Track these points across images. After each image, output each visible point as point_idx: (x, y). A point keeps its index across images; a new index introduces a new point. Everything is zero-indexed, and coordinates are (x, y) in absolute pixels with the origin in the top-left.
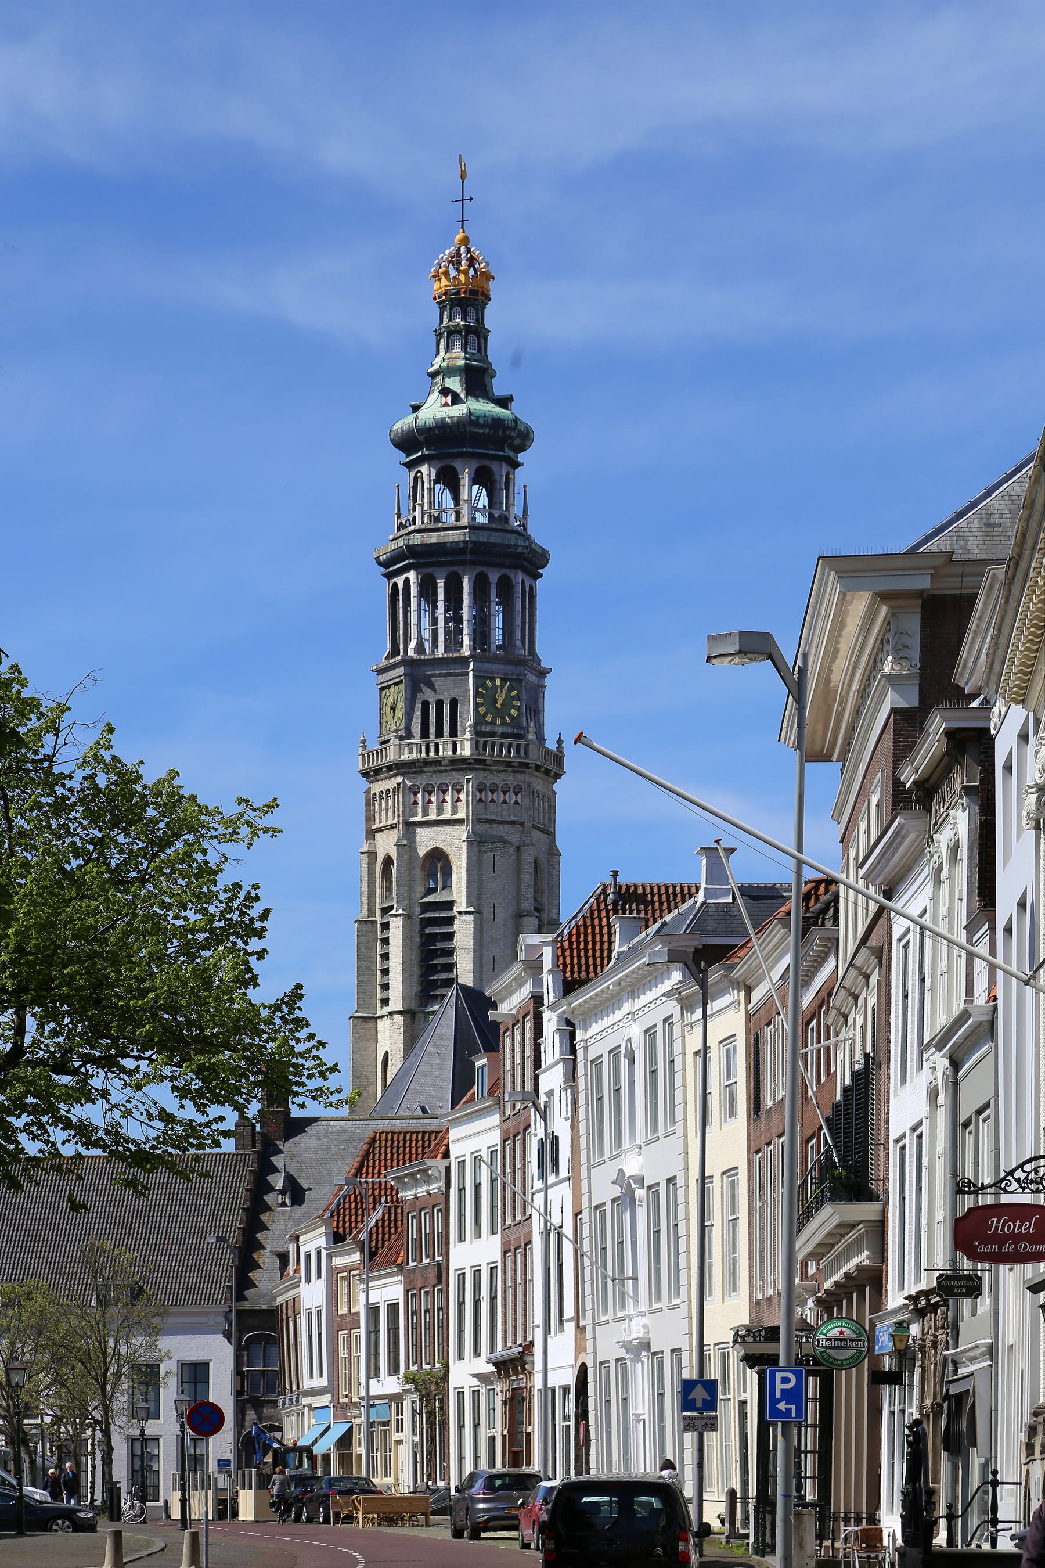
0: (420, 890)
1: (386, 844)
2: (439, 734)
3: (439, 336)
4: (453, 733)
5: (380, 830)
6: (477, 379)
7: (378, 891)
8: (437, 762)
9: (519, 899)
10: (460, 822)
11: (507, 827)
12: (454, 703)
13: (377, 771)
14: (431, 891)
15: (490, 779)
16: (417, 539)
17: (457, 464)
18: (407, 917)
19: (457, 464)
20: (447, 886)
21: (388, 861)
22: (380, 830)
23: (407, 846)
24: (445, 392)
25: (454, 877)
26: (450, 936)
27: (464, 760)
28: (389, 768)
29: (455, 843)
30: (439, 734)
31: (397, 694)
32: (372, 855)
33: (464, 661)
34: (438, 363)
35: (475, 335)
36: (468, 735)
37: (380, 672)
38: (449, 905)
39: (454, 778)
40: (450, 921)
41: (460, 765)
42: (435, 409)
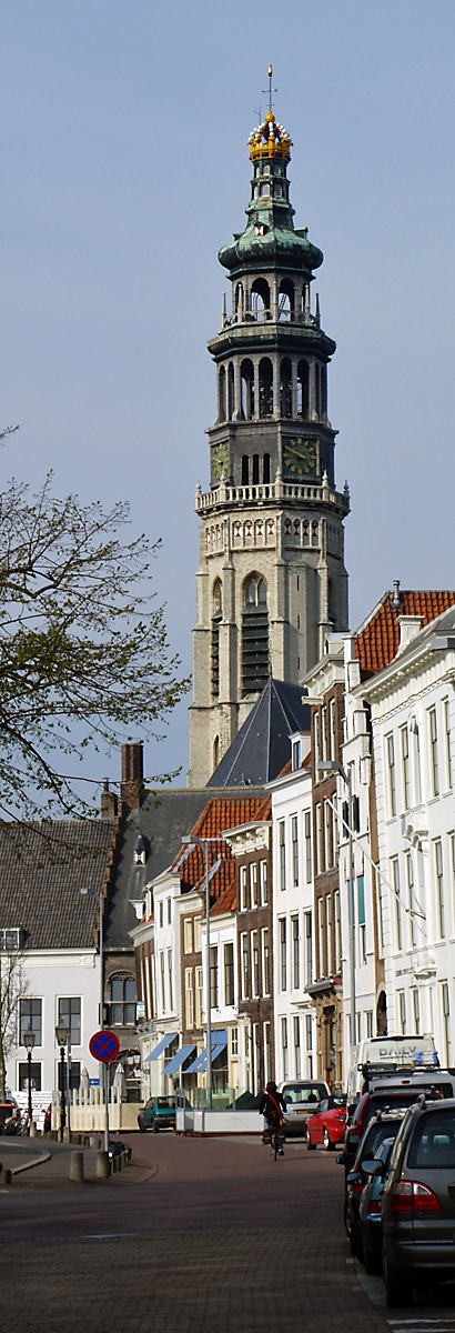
3: (254, 184)
6: (282, 216)
10: (273, 549)
12: (267, 457)
13: (209, 511)
16: (238, 333)
21: (218, 582)
28: (219, 508)
29: (268, 565)
33: (274, 424)
35: (280, 185)
37: (210, 433)
42: (254, 238)
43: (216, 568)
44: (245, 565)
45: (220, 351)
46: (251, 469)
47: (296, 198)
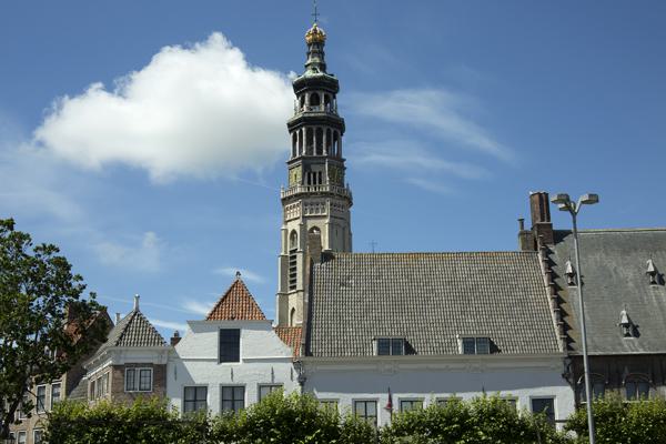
1: (295, 226)
2: (315, 183)
3: (309, 54)
4: (320, 182)
6: (323, 67)
10: (325, 216)
12: (320, 173)
13: (290, 198)
15: (334, 201)
21: (294, 232)
23: (303, 226)
24: (314, 69)
27: (326, 193)
28: (296, 195)
30: (315, 183)
31: (298, 171)
32: (286, 230)
33: (324, 158)
34: (309, 61)
35: (321, 54)
37: (289, 163)
41: (325, 195)
42: (309, 74)
43: (295, 226)
44: (310, 224)
45: (293, 126)
46: (310, 176)
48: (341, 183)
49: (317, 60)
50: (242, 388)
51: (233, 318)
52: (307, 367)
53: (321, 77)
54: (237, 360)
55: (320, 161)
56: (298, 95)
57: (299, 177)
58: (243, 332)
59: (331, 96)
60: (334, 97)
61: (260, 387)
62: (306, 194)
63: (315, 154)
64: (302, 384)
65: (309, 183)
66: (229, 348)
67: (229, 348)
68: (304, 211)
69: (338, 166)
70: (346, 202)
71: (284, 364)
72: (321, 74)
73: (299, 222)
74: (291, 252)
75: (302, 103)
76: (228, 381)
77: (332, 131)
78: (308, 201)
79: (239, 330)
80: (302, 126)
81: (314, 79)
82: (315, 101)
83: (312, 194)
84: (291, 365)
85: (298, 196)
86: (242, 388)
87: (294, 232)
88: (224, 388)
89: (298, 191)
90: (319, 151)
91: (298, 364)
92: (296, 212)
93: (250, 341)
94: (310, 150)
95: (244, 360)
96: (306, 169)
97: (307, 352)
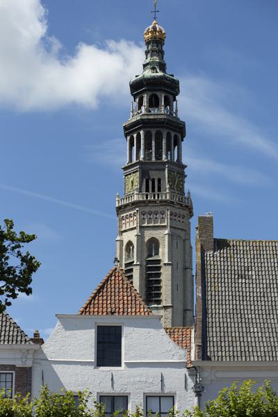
0: (146, 254)
1: (131, 236)
2: (153, 190)
4: (159, 190)
5: (125, 231)
6: (162, 67)
7: (124, 257)
8: (155, 202)
9: (185, 261)
10: (164, 227)
11: (180, 231)
12: (159, 180)
13: (126, 206)
14: (150, 255)
15: (175, 211)
16: (146, 117)
17: (158, 94)
18: (141, 265)
19: (158, 94)
20: (157, 253)
21: (130, 243)
22: (125, 231)
23: (140, 237)
24: (153, 69)
25: (160, 250)
26: (159, 275)
27: (165, 201)
28: (133, 204)
29: (163, 236)
30: (153, 190)
31: (135, 177)
32: (121, 241)
34: (148, 61)
35: (160, 53)
36: (168, 191)
37: (125, 169)
38: (159, 261)
39: (161, 208)
40: (159, 268)
41: (165, 203)
43: (131, 236)
44: (148, 235)
45: (129, 130)
46: (149, 183)
47: (167, 59)
48: (182, 191)
49: (157, 59)
50: (125, 398)
51: (112, 313)
52: (205, 374)
53: (161, 77)
54: (119, 364)
55: (160, 166)
56: (135, 97)
57: (137, 184)
58: (126, 331)
59: (171, 97)
60: (175, 100)
61: (147, 397)
62: (144, 202)
63: (154, 159)
64: (198, 394)
65: (147, 190)
66: (108, 349)
67: (108, 349)
68: (142, 220)
69: (178, 171)
70: (186, 212)
71: (174, 370)
72: (160, 74)
73: (135, 232)
74: (127, 265)
75: (140, 104)
76: (107, 389)
77: (173, 134)
78: (147, 209)
79: (120, 327)
80: (140, 129)
81: (154, 78)
82: (154, 103)
83: (150, 202)
84: (185, 371)
85: (135, 204)
86: (125, 398)
87: (130, 243)
88: (102, 398)
89: (136, 198)
90: (159, 156)
91: (194, 370)
92: (133, 222)
93: (135, 341)
94: (148, 155)
95: (129, 365)
96: (144, 175)
97: (204, 353)
